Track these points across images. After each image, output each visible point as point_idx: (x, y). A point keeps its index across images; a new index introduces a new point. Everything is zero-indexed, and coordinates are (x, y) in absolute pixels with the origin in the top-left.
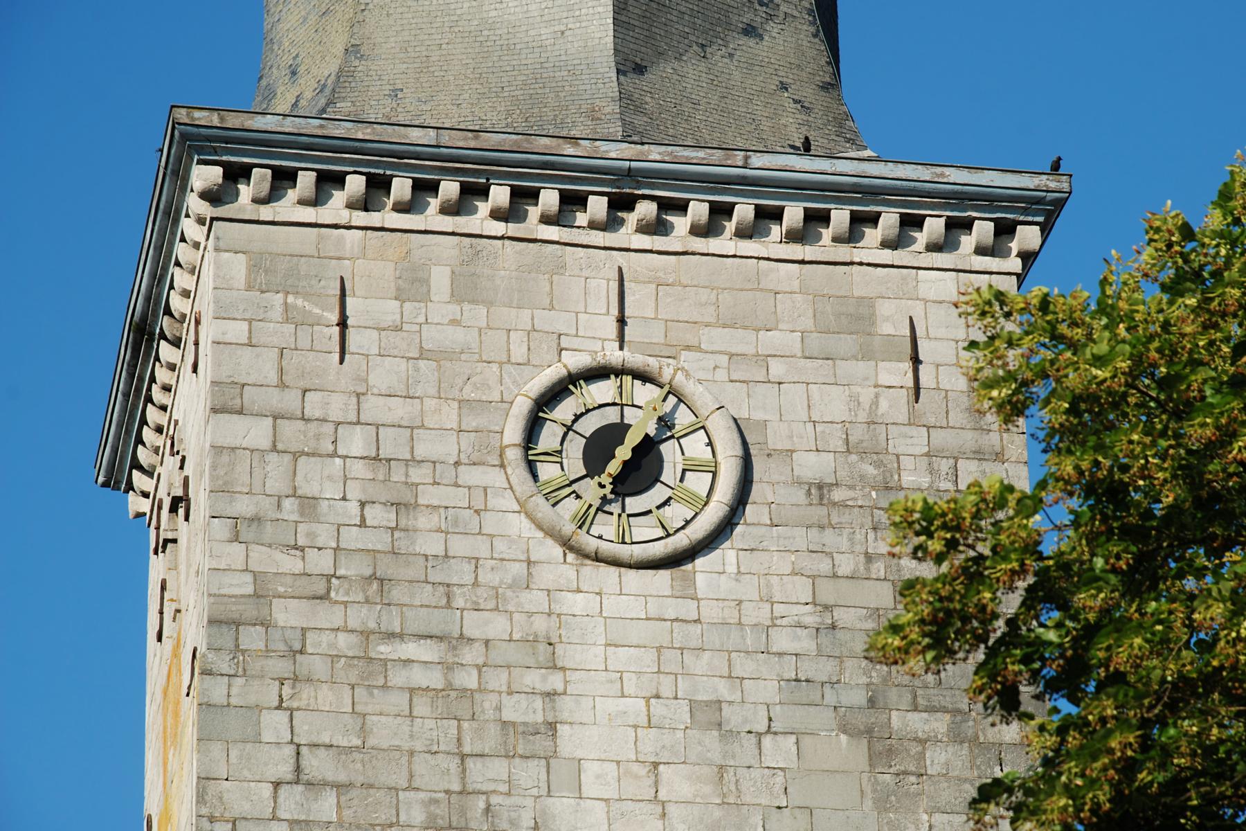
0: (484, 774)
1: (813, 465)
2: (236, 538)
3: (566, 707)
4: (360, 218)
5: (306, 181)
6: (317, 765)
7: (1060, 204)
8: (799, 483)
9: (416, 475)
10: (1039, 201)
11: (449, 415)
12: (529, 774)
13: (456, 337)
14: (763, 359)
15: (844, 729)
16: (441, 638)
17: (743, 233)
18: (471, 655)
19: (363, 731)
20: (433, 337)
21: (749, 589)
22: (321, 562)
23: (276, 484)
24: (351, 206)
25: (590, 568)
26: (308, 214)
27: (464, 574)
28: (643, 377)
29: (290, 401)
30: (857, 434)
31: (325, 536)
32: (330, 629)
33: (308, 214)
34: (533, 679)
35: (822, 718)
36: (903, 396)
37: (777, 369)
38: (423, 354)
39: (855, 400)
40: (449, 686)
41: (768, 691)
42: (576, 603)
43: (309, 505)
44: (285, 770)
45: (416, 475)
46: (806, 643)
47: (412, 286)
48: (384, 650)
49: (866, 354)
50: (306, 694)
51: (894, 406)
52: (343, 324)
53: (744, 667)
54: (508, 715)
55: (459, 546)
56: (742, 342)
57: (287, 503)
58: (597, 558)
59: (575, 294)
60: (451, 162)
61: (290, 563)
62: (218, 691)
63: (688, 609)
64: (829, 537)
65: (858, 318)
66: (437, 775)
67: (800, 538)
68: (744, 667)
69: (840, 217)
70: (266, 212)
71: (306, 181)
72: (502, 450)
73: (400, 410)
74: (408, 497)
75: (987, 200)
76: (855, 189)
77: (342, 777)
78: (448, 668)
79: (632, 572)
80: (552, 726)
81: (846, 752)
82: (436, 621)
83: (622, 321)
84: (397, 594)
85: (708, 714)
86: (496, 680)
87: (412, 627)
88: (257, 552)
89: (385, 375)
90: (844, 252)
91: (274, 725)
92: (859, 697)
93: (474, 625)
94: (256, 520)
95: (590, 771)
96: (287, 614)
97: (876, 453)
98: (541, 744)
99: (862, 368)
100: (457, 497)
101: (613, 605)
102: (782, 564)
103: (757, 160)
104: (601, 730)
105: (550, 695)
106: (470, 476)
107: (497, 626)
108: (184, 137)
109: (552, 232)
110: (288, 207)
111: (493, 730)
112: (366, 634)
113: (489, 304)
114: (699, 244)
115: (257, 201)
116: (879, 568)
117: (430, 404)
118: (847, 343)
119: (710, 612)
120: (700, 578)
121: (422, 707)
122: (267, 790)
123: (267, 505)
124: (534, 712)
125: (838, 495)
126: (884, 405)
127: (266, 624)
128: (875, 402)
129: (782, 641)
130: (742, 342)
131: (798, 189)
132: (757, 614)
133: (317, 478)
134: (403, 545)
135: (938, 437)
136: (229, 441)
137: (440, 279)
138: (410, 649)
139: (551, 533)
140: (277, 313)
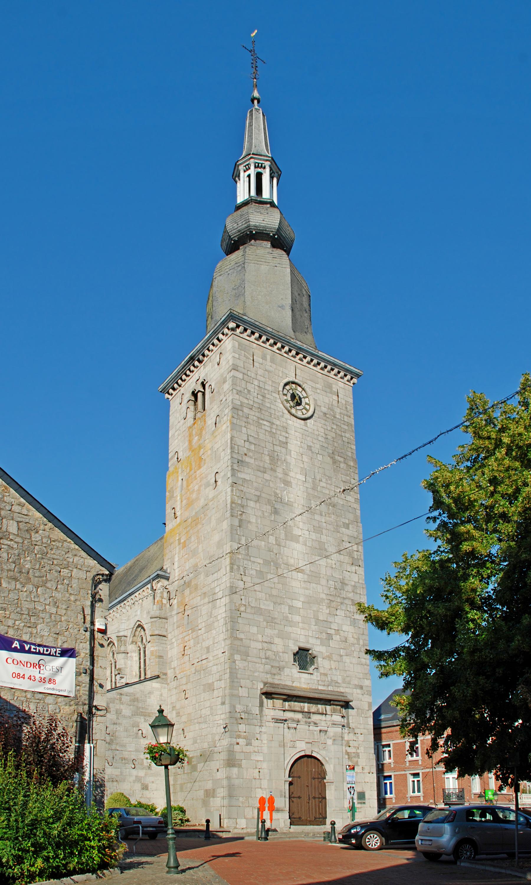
0: (277, 448)
1: (324, 410)
2: (237, 394)
3: (289, 439)
4: (256, 342)
5: (249, 331)
6: (251, 439)
7: (360, 376)
8: (322, 412)
9: (266, 392)
10: (358, 375)
11: (270, 383)
12: (284, 450)
13: (271, 369)
14: (316, 389)
15: (329, 456)
16: (270, 422)
17: (314, 366)
18: (274, 427)
19: (258, 435)
20: (268, 368)
21: (315, 428)
22: (251, 403)
23: (244, 386)
24: (255, 339)
25: (292, 416)
26: (248, 338)
27: (273, 412)
28: (300, 386)
29: (246, 372)
30: (330, 406)
31: (251, 398)
32: (253, 415)
33: (248, 338)
34: (284, 434)
35: (326, 454)
36: (337, 402)
37: (318, 391)
38: (266, 370)
39: (329, 400)
40: (271, 431)
41: (318, 446)
42: (290, 422)
43: (249, 391)
44: (246, 439)
45: (266, 392)
46: (323, 440)
47: (264, 358)
48: (261, 421)
49: (331, 393)
50: (249, 426)
51: (335, 403)
52: (253, 360)
53: (315, 441)
54: (280, 439)
55: (272, 406)
56: (314, 385)
57: (246, 390)
58: (293, 415)
59: (292, 368)
60: (273, 336)
61: (246, 401)
62: (235, 421)
63: (304, 428)
64: (326, 423)
65: (329, 386)
66: (269, 446)
67: (323, 422)
68: (315, 441)
69: (329, 367)
70: (241, 335)
71: (249, 331)
72: (279, 392)
73: (262, 379)
74: (264, 395)
75: (351, 372)
76: (333, 363)
77: (255, 443)
78: (271, 428)
79: (298, 420)
80: (287, 443)
81: (329, 460)
82: (268, 418)
83: (296, 374)
84: (263, 412)
85: (309, 448)
86: (278, 432)
87: (266, 419)
88: (241, 397)
89: (260, 372)
90: (328, 374)
91: (244, 430)
92: (331, 452)
93: (275, 421)
94: (240, 391)
95: (293, 453)
96: (246, 410)
97: (332, 410)
98: (285, 445)
99: (330, 395)
100: (272, 398)
101: (296, 424)
102: (320, 425)
103: (320, 353)
104: (294, 445)
105: (286, 437)
106: (274, 394)
107: (278, 423)
108: (231, 316)
109: (285, 355)
110: (245, 335)
111: (278, 441)
112: (258, 418)
113: (276, 365)
114: (307, 365)
115: (240, 333)
116: (333, 430)
117: (267, 379)
118: (328, 390)
119: (310, 430)
120: (308, 424)
121: (267, 434)
122: (243, 442)
123: (242, 389)
124: (284, 440)
125: (328, 416)
126: (334, 403)
127: (242, 411)
128: (332, 402)
129: (320, 438)
130: (314, 385)
131: (324, 360)
132: (317, 433)
133: (250, 387)
134: (264, 404)
135: (342, 411)
136: (236, 376)
137: (268, 357)
138: (265, 423)
139: (286, 409)
140: (243, 355)
